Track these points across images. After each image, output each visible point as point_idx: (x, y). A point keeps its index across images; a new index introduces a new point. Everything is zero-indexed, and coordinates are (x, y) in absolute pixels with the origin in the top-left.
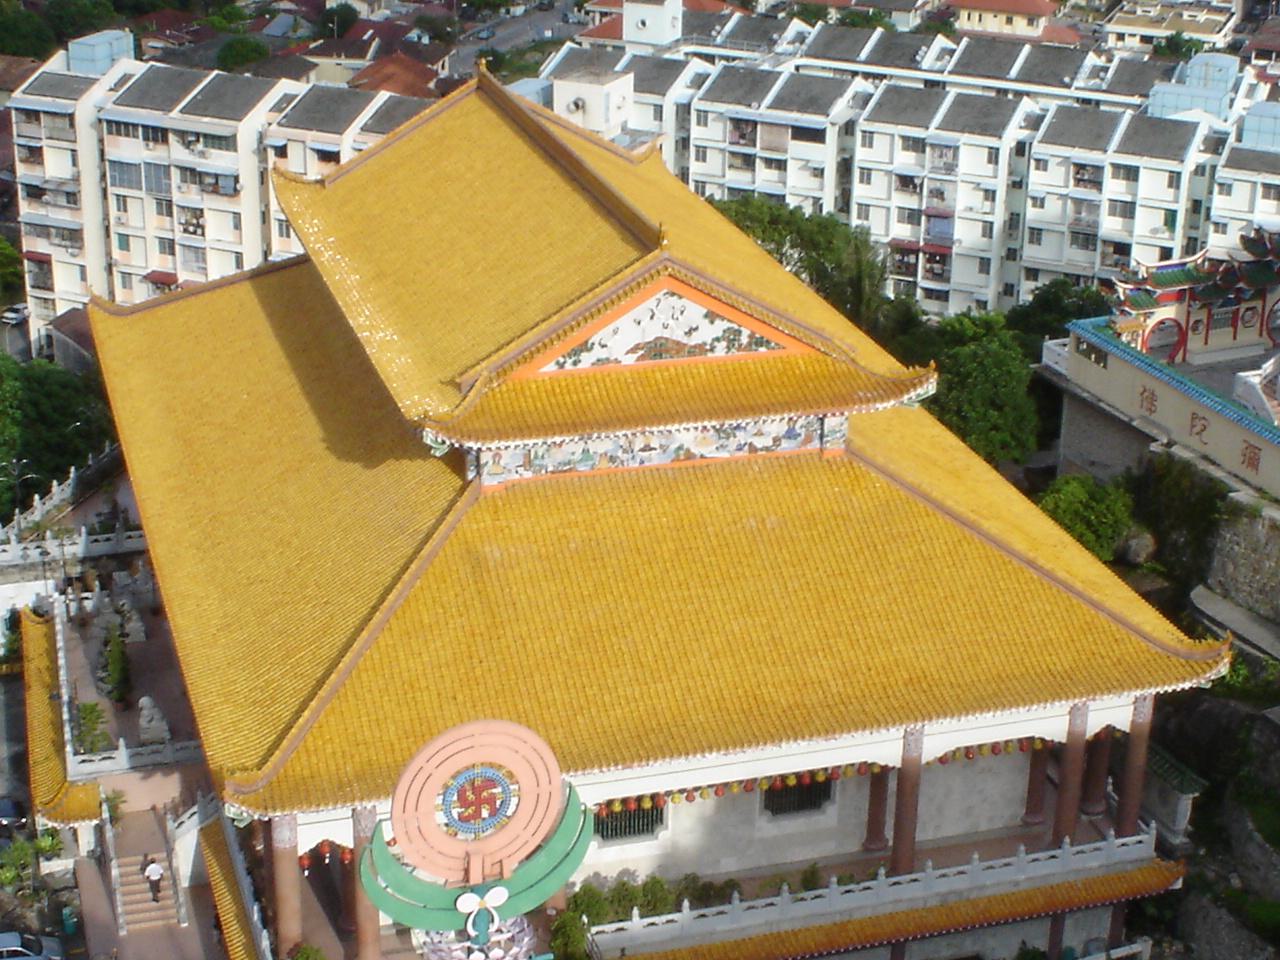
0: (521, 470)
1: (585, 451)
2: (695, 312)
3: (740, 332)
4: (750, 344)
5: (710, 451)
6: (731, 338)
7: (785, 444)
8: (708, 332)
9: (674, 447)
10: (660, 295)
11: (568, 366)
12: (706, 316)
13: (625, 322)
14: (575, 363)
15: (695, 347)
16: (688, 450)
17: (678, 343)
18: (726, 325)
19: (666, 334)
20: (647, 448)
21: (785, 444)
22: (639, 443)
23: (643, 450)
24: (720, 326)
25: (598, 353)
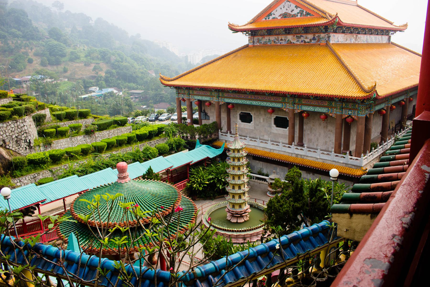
1: (269, 39)
2: (293, 6)
3: (303, 11)
4: (306, 14)
5: (295, 42)
6: (301, 13)
7: (313, 41)
9: (287, 40)
10: (285, 2)
11: (267, 19)
12: (295, 7)
13: (278, 9)
14: (269, 18)
15: (293, 15)
17: (290, 14)
18: (300, 9)
19: (287, 11)
20: (282, 40)
21: (313, 41)
22: (280, 39)
23: (281, 40)
24: (299, 9)
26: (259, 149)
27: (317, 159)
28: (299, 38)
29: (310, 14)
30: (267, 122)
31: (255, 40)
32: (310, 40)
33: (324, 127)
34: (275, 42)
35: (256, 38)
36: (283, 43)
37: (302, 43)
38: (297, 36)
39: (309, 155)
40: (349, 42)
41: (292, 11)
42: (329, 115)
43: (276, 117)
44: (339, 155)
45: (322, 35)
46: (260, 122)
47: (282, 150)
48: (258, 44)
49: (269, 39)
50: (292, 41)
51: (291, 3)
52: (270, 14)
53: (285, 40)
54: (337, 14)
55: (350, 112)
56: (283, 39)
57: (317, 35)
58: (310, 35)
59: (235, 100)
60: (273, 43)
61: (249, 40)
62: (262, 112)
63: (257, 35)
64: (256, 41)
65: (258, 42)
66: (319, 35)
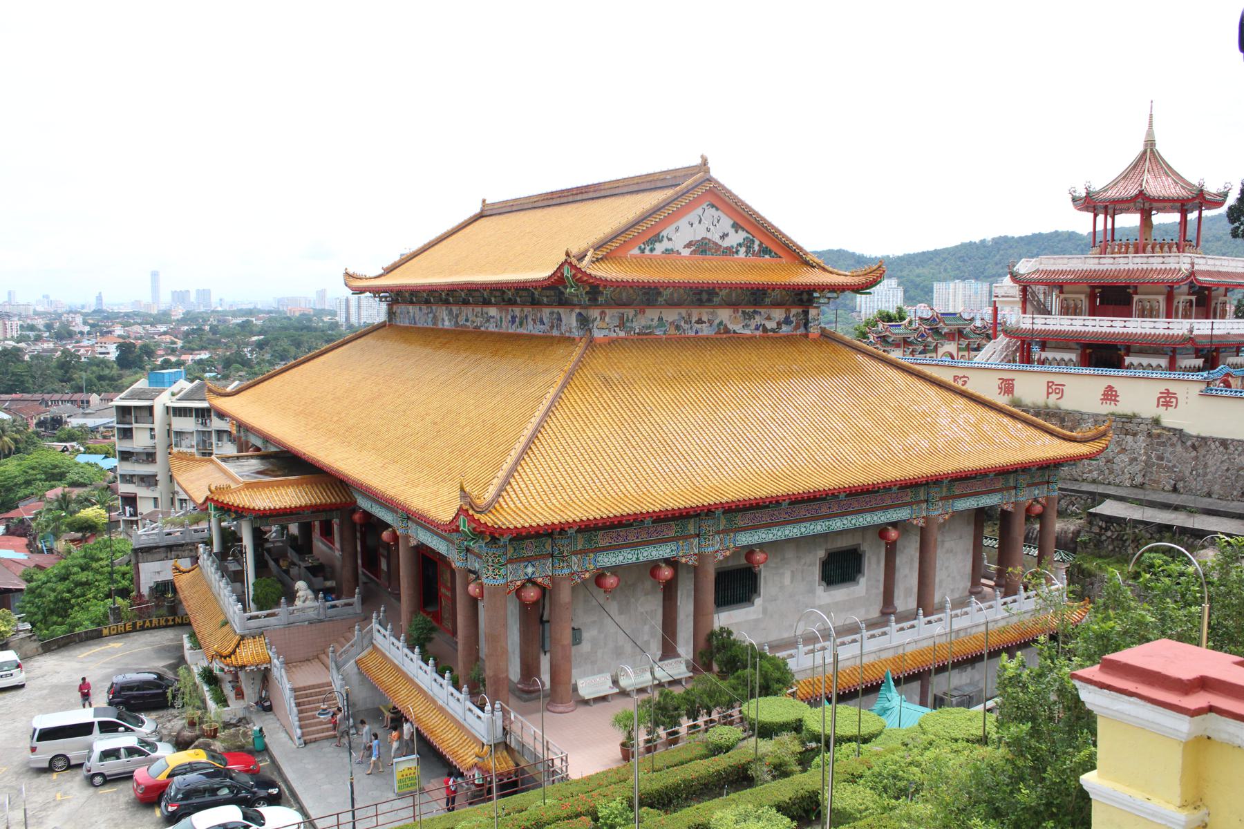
0: (617, 329)
1: (660, 319)
2: (726, 223)
5: (738, 328)
6: (748, 244)
7: (785, 329)
8: (735, 238)
11: (647, 252)
12: (733, 226)
13: (683, 223)
14: (652, 250)
18: (744, 235)
19: (709, 236)
20: (700, 321)
22: (694, 319)
23: (697, 322)
25: (666, 244)
28: (749, 316)
29: (770, 251)
30: (803, 579)
32: (779, 324)
34: (678, 327)
36: (706, 330)
38: (743, 312)
41: (724, 236)
48: (622, 334)
50: (730, 327)
51: (719, 213)
52: (657, 239)
53: (711, 322)
56: (705, 319)
60: (672, 331)
62: (790, 554)
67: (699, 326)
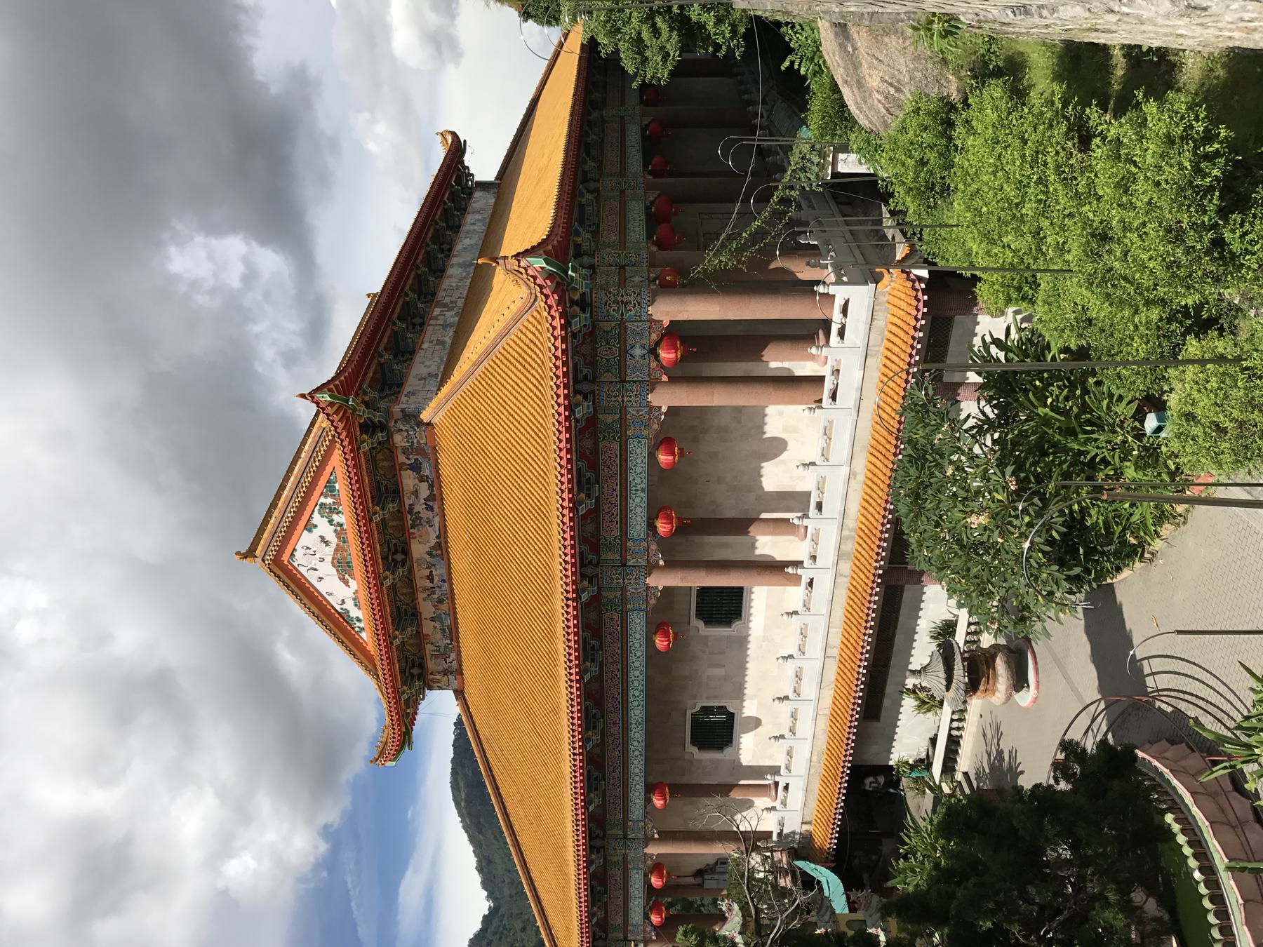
1: (433, 619)
2: (307, 539)
4: (333, 496)
5: (432, 534)
7: (426, 471)
8: (323, 527)
9: (429, 559)
11: (362, 625)
13: (322, 588)
14: (359, 620)
15: (338, 538)
16: (433, 548)
17: (336, 550)
18: (316, 516)
19: (329, 559)
20: (430, 577)
22: (429, 584)
23: (432, 581)
24: (317, 518)
25: (349, 605)
26: (827, 702)
27: (851, 475)
31: (440, 668)
32: (422, 479)
33: (725, 440)
34: (440, 601)
35: (431, 664)
37: (436, 508)
39: (840, 507)
40: (451, 332)
41: (327, 543)
42: (658, 433)
43: (699, 615)
44: (828, 385)
45: (399, 440)
46: (726, 678)
47: (824, 610)
49: (433, 619)
50: (433, 542)
52: (344, 615)
53: (430, 565)
54: (303, 396)
55: (638, 352)
56: (427, 572)
57: (402, 459)
58: (405, 482)
59: (632, 783)
61: (440, 688)
63: (422, 658)
64: (442, 665)
65: (444, 656)
66: (399, 450)
67: (436, 579)
